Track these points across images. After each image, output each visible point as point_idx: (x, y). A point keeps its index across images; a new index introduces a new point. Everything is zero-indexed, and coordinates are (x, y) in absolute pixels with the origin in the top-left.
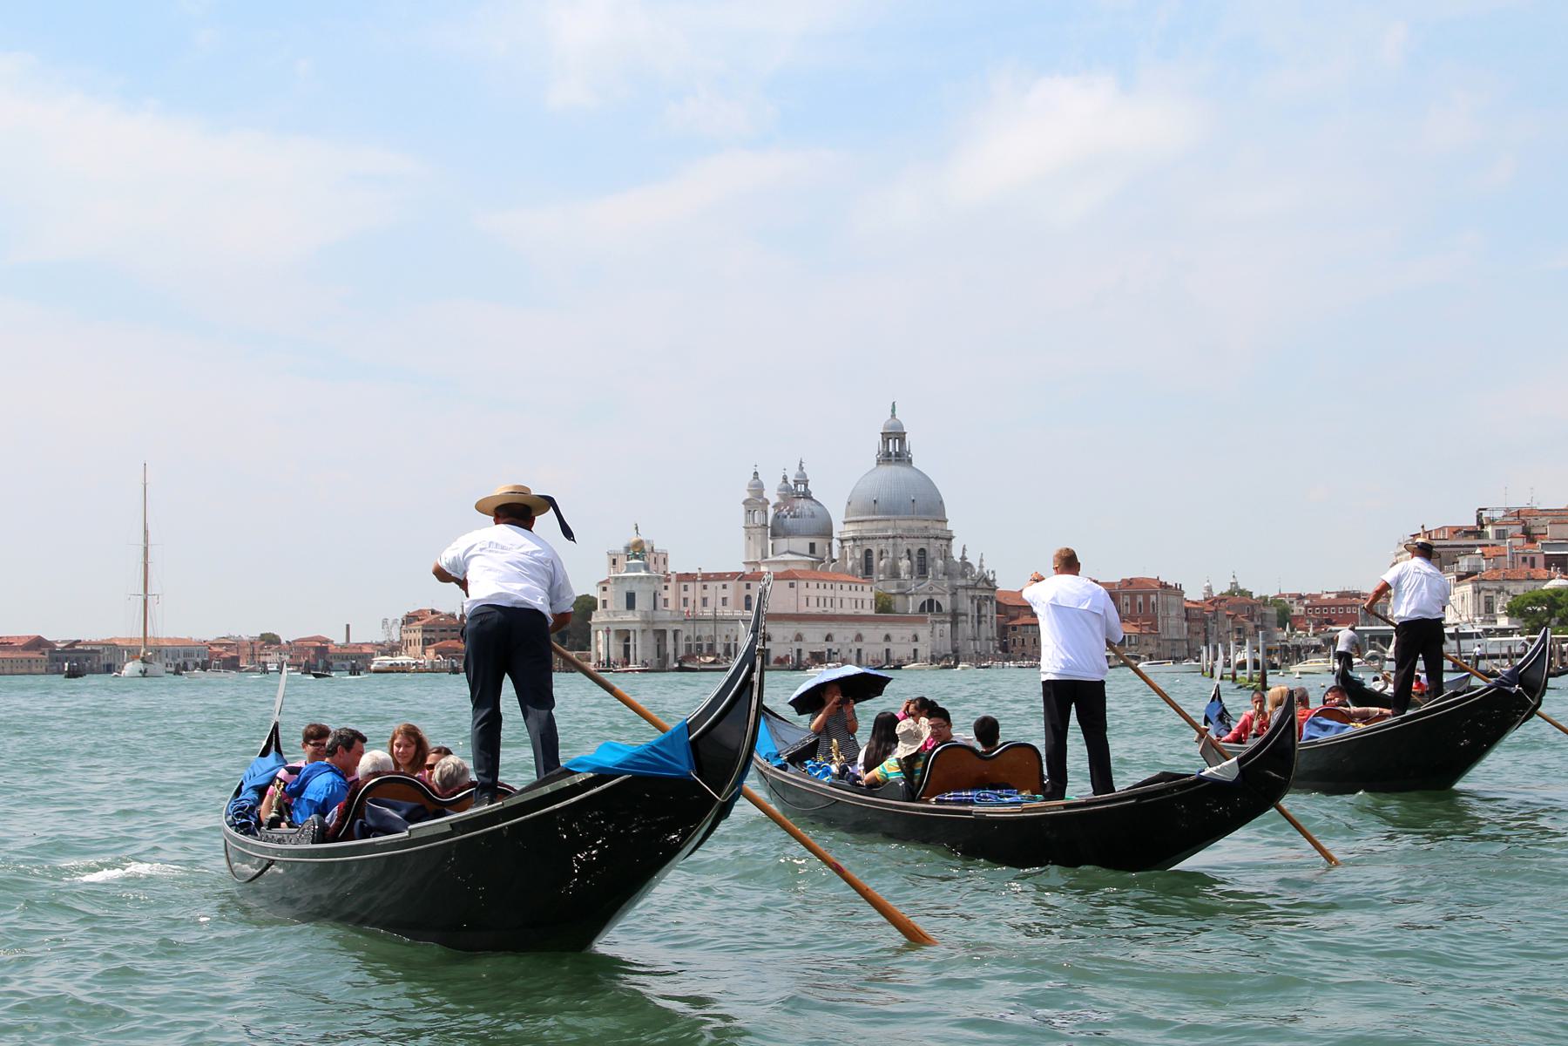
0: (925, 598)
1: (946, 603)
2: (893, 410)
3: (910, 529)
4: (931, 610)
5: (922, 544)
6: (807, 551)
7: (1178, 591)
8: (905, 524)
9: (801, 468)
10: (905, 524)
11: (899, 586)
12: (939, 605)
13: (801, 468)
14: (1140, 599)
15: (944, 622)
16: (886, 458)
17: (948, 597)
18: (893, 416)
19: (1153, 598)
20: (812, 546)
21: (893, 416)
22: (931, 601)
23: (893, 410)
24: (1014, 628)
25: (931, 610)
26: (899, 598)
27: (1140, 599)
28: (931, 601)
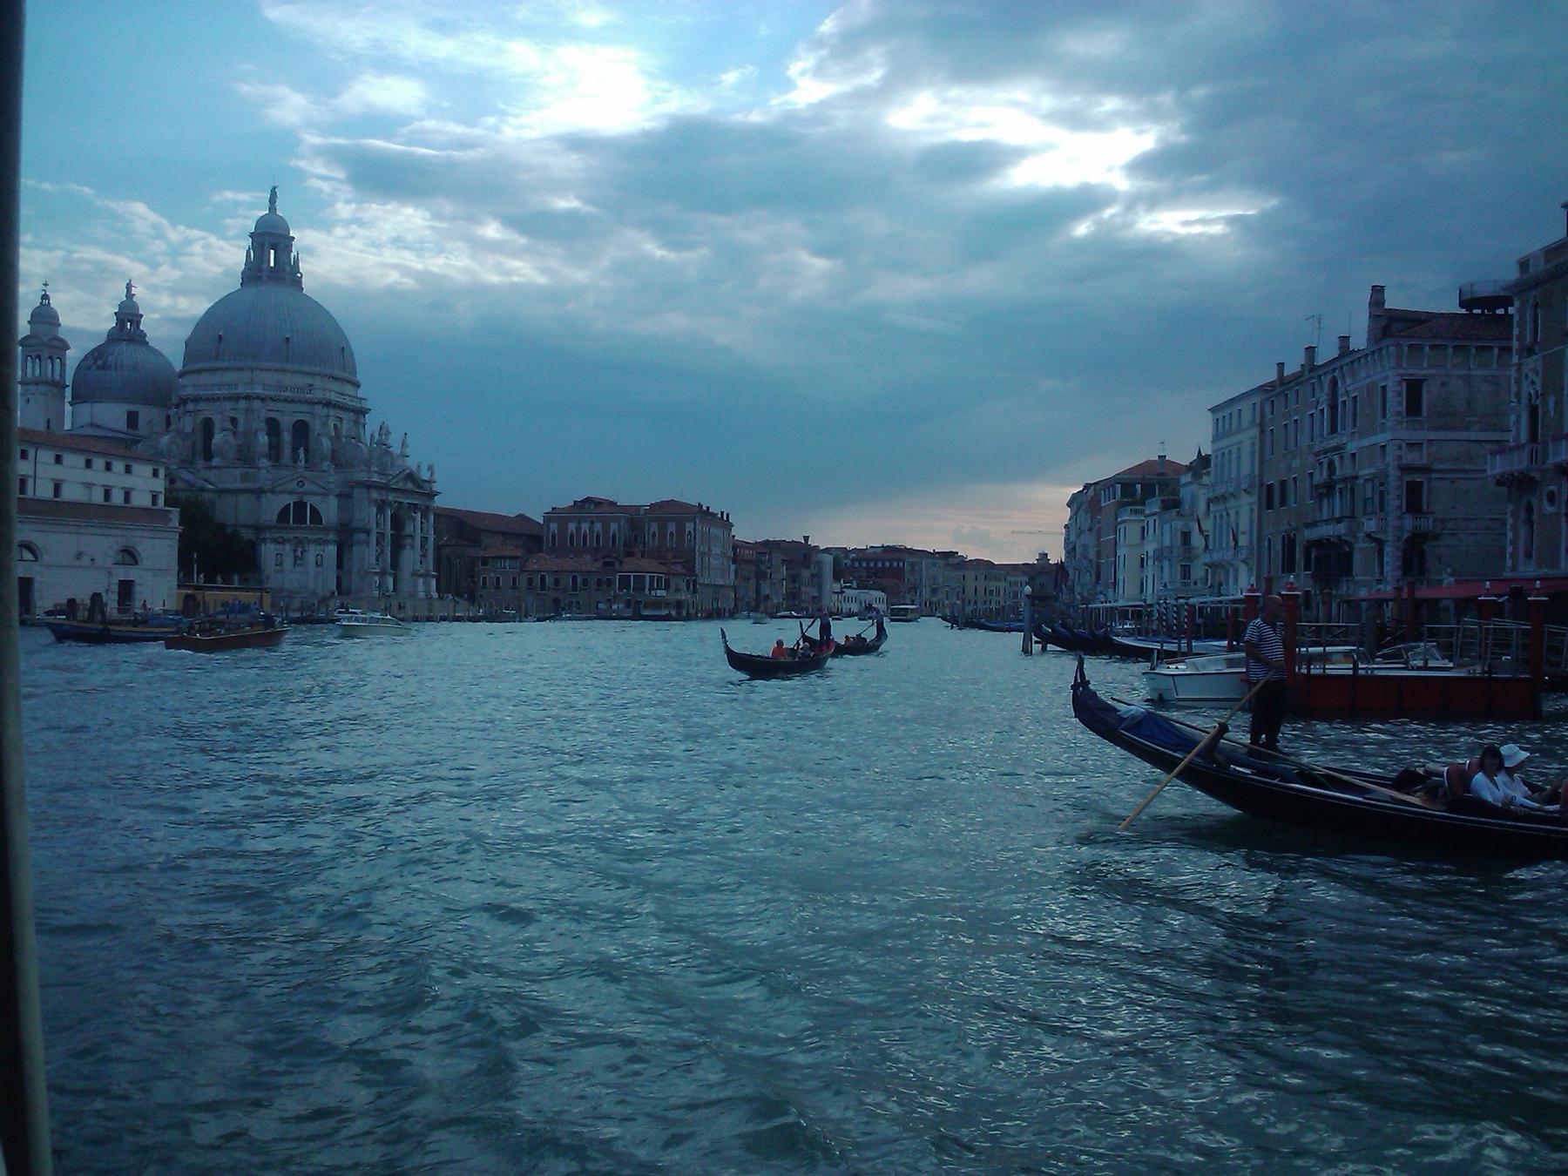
1: (330, 510)
2: (273, 200)
3: (280, 387)
4: (300, 519)
9: (129, 295)
11: (244, 478)
13: (129, 295)
14: (672, 527)
15: (326, 542)
16: (254, 273)
17: (333, 503)
18: (272, 208)
20: (132, 419)
21: (272, 208)
22: (300, 506)
23: (273, 200)
26: (243, 498)
27: (672, 527)
28: (300, 506)
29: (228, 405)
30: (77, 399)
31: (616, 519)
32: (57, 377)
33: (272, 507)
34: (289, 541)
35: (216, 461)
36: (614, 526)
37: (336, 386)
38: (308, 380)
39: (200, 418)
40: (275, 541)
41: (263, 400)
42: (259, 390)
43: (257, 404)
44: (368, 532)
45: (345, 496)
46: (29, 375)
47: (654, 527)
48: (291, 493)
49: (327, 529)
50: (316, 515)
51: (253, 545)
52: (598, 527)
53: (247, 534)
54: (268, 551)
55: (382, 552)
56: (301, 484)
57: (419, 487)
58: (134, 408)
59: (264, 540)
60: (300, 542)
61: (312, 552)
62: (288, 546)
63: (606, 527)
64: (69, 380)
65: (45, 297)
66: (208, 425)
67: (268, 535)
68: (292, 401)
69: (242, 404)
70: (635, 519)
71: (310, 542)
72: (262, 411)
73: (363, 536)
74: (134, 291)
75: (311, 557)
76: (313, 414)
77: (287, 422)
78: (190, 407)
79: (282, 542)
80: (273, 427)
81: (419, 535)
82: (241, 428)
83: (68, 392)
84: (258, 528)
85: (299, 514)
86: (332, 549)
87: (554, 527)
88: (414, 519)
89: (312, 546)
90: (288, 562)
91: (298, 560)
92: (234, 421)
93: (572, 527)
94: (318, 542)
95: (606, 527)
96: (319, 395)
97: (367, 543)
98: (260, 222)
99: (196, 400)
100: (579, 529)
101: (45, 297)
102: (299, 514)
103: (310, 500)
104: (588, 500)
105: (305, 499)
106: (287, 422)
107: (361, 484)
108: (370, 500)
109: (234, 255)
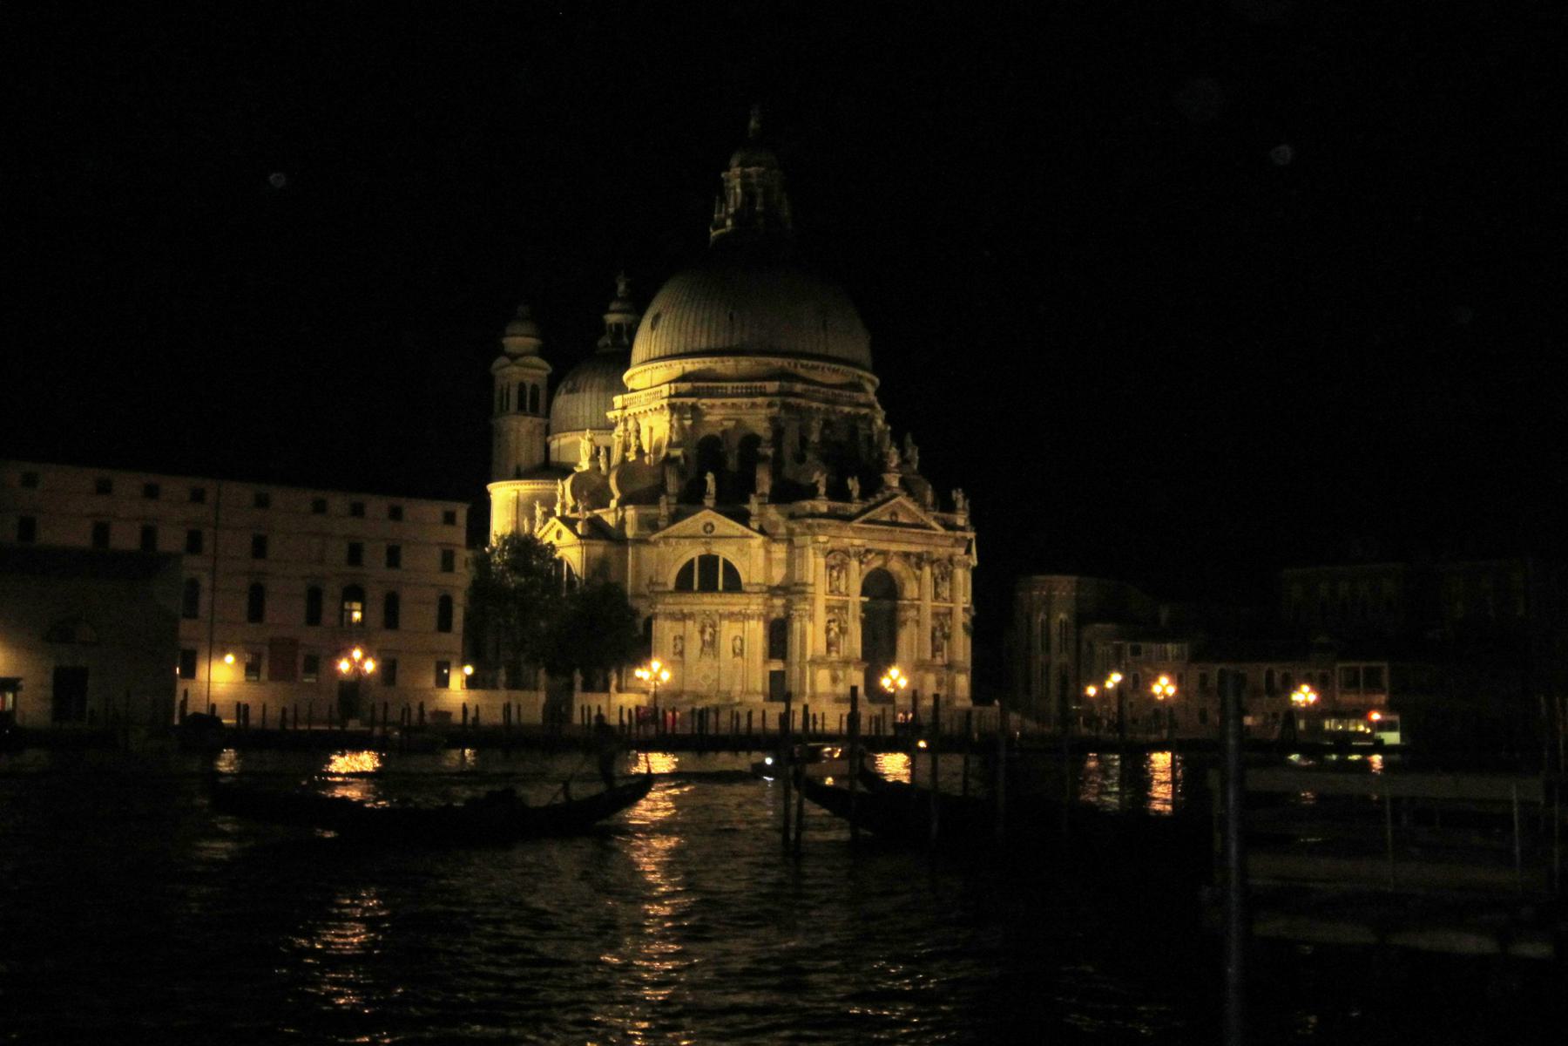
0: (693, 552)
12: (729, 568)
15: (746, 617)
22: (709, 562)
25: (709, 586)
28: (709, 562)
34: (691, 616)
40: (672, 616)
55: (843, 631)
61: (729, 632)
62: (690, 623)
81: (928, 604)
89: (725, 623)
90: (694, 647)
94: (731, 616)
97: (812, 617)
103: (725, 552)
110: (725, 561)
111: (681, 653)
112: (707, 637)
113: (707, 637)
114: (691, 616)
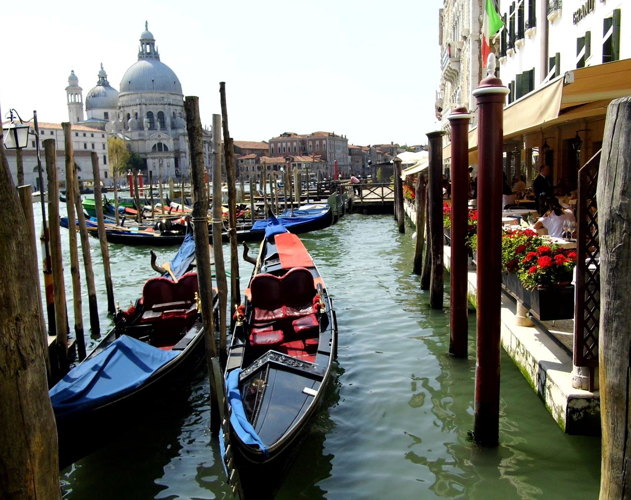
0: (156, 142)
1: (170, 145)
2: (146, 26)
5: (160, 108)
6: (103, 117)
7: (345, 140)
8: (149, 95)
9: (102, 68)
10: (149, 95)
11: (140, 135)
12: (165, 146)
13: (102, 68)
14: (317, 143)
16: (142, 56)
18: (147, 29)
19: (324, 142)
20: (106, 114)
21: (147, 29)
22: (160, 145)
23: (146, 26)
24: (242, 161)
25: (160, 150)
26: (140, 142)
27: (317, 143)
28: (160, 145)
29: (134, 108)
30: (88, 109)
31: (296, 141)
32: (80, 101)
33: (149, 145)
34: (157, 158)
35: (130, 130)
36: (295, 144)
37: (174, 97)
38: (162, 95)
39: (126, 113)
40: (152, 158)
41: (146, 105)
42: (144, 100)
43: (144, 106)
44: (185, 153)
45: (176, 139)
46: (70, 101)
47: (311, 143)
48: (156, 139)
49: (170, 152)
50: (166, 148)
51: (145, 160)
52: (289, 144)
53: (142, 156)
54: (150, 162)
56: (159, 136)
57: (206, 134)
58: (106, 111)
59: (148, 158)
60: (161, 158)
61: (165, 161)
62: (156, 160)
63: (292, 144)
64: (84, 102)
65: (73, 71)
66: (129, 117)
67: (149, 156)
68: (156, 104)
69: (138, 106)
70: (303, 141)
71: (164, 158)
72: (145, 110)
73: (184, 155)
74: (103, 66)
75: (165, 164)
76: (164, 109)
77: (155, 113)
78: (122, 109)
79: (155, 158)
80: (150, 115)
82: (139, 115)
83: (84, 107)
84: (146, 154)
85: (160, 147)
86: (173, 160)
87: (272, 145)
88: (205, 147)
89: (165, 159)
90: (157, 166)
91: (161, 165)
92: (136, 114)
93: (279, 145)
94: (167, 157)
95: (292, 144)
96: (166, 101)
97: (186, 157)
98: (143, 35)
99: (123, 107)
100: (282, 145)
101: (73, 71)
102: (160, 147)
103: (163, 142)
104: (285, 134)
105: (162, 142)
106: (155, 113)
107: (181, 134)
108: (185, 141)
109: (137, 47)
110: (164, 144)
111: (155, 167)
112: (161, 162)
113: (161, 162)
114: (157, 158)
